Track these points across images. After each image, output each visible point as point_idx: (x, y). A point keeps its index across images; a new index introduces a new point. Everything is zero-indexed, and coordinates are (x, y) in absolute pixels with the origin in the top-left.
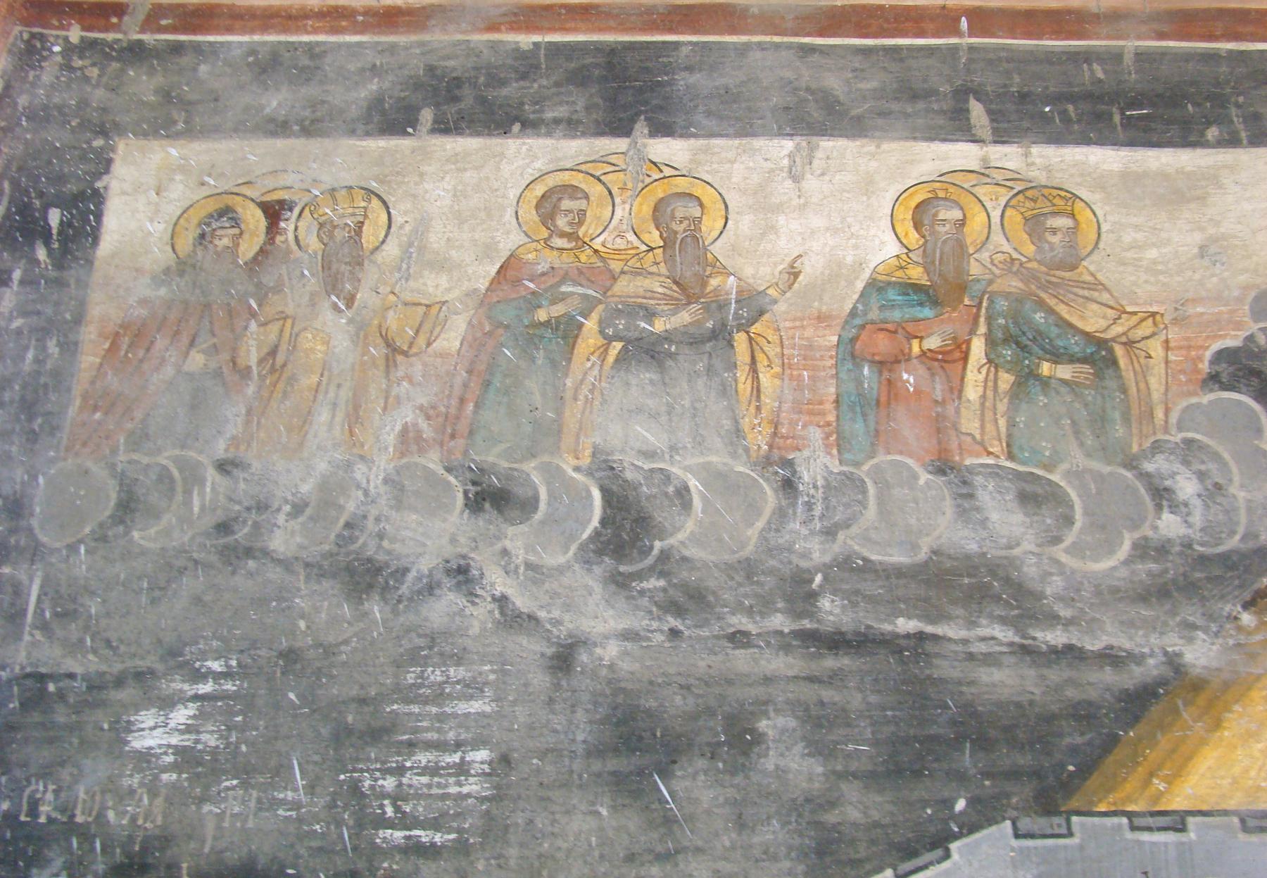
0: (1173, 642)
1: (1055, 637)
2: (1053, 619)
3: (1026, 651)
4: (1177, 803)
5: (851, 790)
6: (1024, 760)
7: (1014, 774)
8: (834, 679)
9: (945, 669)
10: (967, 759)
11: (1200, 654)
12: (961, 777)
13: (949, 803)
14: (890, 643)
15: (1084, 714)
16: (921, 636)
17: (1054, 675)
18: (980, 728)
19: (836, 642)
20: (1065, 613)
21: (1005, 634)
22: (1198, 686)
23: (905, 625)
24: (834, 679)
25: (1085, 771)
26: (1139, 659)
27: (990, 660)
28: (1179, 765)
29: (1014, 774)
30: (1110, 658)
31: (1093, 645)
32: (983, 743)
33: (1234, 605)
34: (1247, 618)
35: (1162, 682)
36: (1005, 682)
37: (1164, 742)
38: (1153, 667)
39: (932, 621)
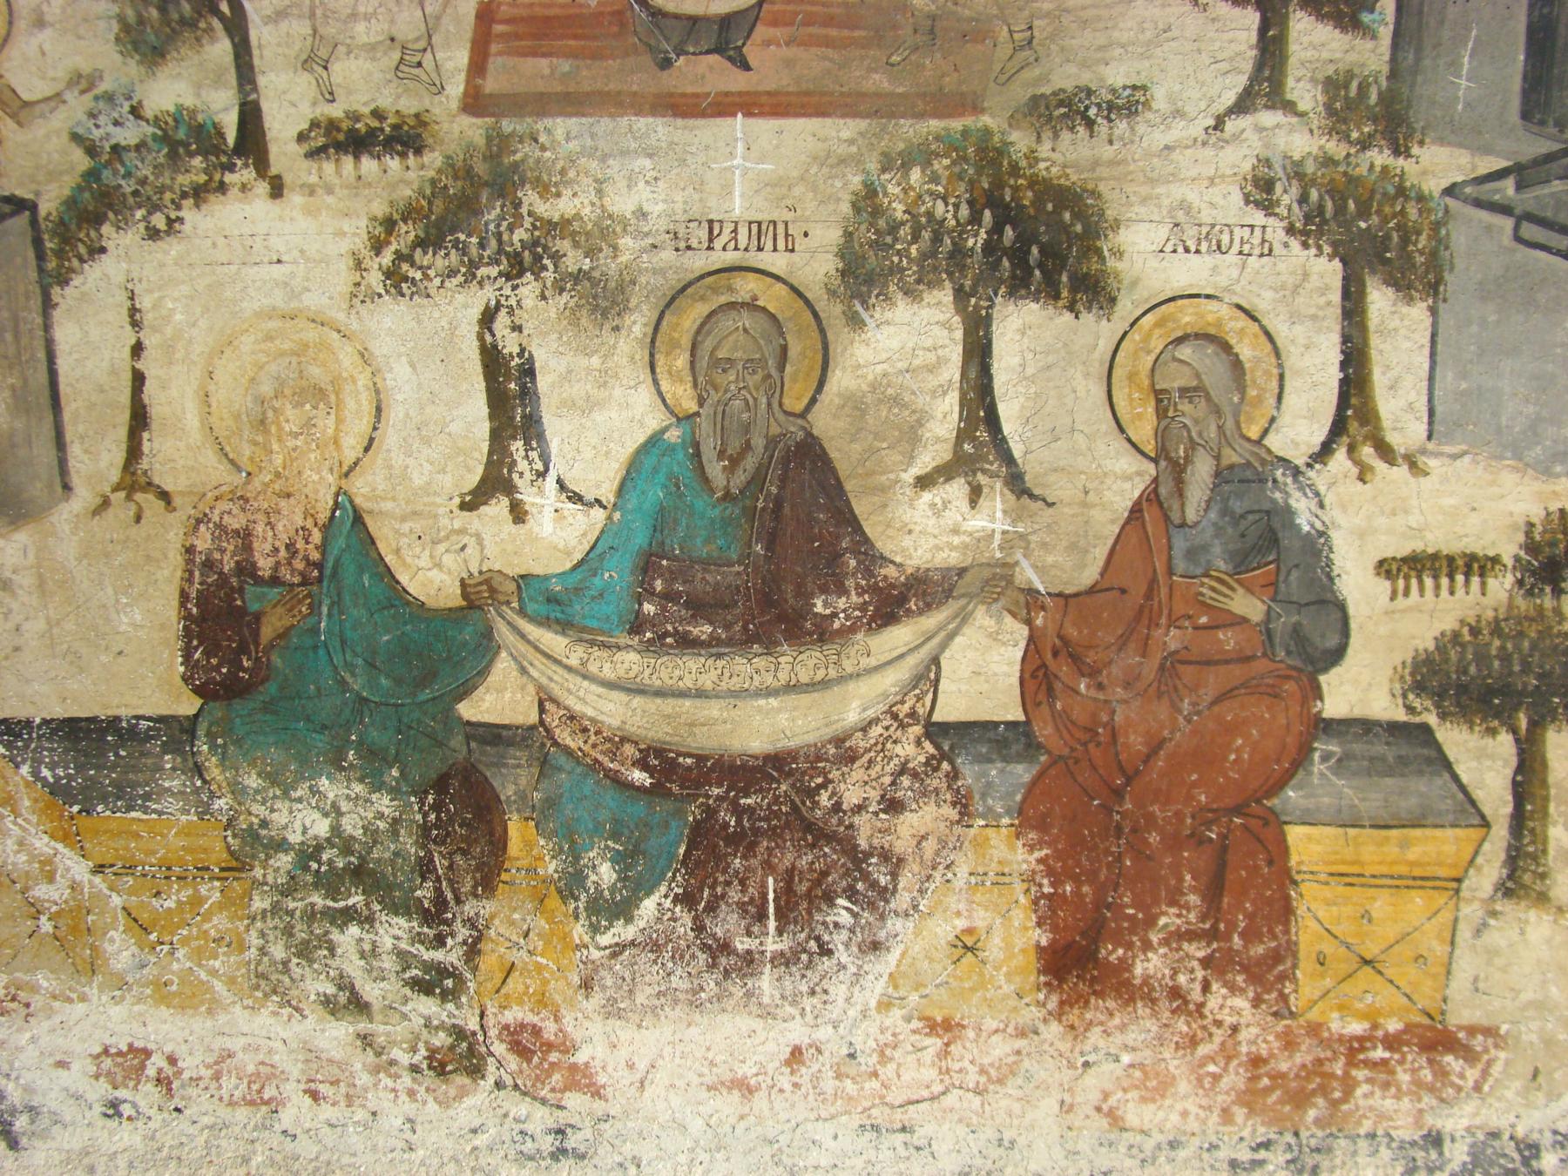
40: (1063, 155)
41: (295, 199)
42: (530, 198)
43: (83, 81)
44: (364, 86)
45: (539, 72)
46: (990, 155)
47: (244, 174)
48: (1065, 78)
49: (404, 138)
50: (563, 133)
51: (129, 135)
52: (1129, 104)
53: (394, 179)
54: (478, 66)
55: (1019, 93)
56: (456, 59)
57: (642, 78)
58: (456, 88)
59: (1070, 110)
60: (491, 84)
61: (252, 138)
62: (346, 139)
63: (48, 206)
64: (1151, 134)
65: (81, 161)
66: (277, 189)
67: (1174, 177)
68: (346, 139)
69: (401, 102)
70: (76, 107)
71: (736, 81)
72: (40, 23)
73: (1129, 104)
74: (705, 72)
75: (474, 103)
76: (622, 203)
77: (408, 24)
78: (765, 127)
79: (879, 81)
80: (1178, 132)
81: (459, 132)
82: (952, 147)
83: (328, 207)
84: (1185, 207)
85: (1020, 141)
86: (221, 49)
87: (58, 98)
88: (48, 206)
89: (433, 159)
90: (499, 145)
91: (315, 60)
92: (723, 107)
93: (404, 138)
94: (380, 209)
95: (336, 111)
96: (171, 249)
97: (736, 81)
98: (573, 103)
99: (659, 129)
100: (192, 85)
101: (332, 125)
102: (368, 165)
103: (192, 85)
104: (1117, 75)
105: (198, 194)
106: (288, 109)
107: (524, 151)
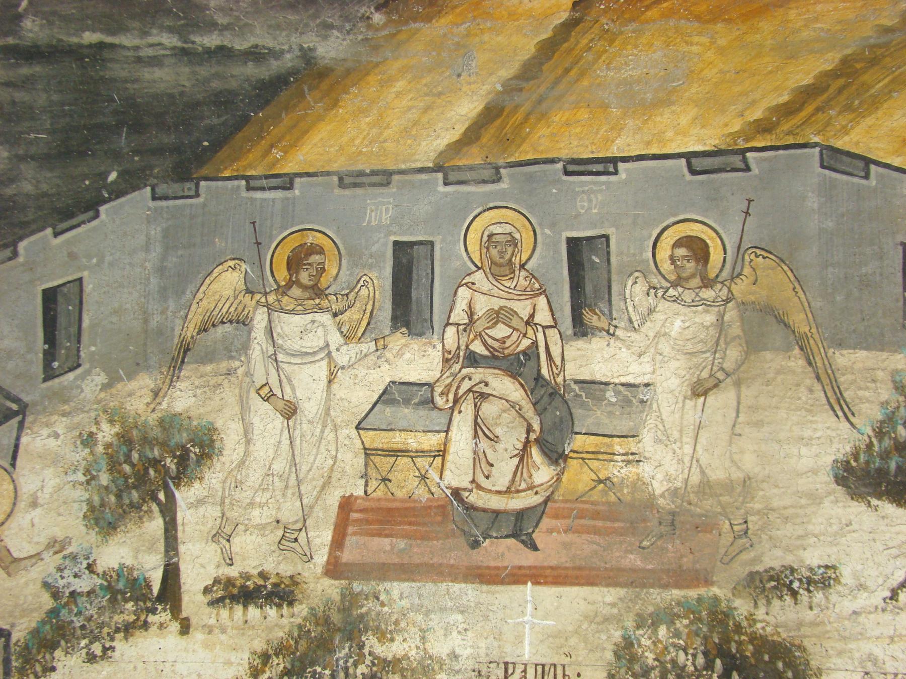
0: (310, 40)
1: (211, 40)
2: (212, 26)
3: (184, 54)
4: (289, 167)
5: (28, 170)
6: (168, 139)
7: (159, 151)
8: (26, 83)
9: (117, 71)
10: (123, 141)
11: (330, 48)
12: (116, 156)
13: (104, 175)
14: (74, 53)
15: (223, 100)
16: (101, 46)
17: (204, 71)
18: (138, 115)
19: (32, 54)
20: (222, 20)
21: (170, 40)
22: (323, 73)
23: (90, 37)
24: (26, 83)
25: (217, 146)
26: (276, 54)
27: (155, 62)
28: (298, 134)
29: (159, 151)
30: (255, 55)
31: (241, 45)
32: (137, 128)
33: (369, 7)
34: (378, 18)
35: (294, 72)
36: (165, 78)
37: (287, 120)
38: (289, 60)
39: (113, 33)
40: (775, 618)
41: (198, 636)
42: (371, 642)
43: (57, 545)
44: (255, 555)
45: (382, 548)
46: (719, 617)
47: (163, 616)
48: (774, 559)
49: (281, 594)
50: (397, 593)
51: (83, 585)
52: (823, 579)
53: (271, 623)
54: (338, 542)
55: (740, 570)
56: (322, 537)
57: (457, 554)
58: (321, 558)
59: (779, 583)
60: (347, 556)
61: (171, 590)
62: (239, 593)
63: (18, 635)
64: (841, 603)
65: (47, 602)
66: (185, 628)
67: (862, 635)
68: (239, 593)
69: (281, 567)
70: (51, 561)
71: (527, 558)
72: (34, 504)
73: (823, 579)
74: (505, 551)
75: (334, 569)
76: (439, 647)
77: (290, 511)
78: (548, 592)
79: (634, 560)
80: (862, 600)
81: (321, 589)
82: (690, 610)
83: (221, 643)
84: (874, 660)
85: (742, 607)
86: (156, 525)
87: (38, 556)
88: (18, 635)
89: (301, 609)
90: (350, 600)
91: (222, 535)
92: (517, 577)
93: (281, 594)
94: (259, 645)
95: (233, 572)
96: (103, 669)
97: (527, 558)
98: (405, 571)
99: (470, 592)
100: (133, 551)
101: (230, 582)
102: (253, 612)
103: (133, 551)
104: (813, 558)
105: (128, 629)
106: (199, 568)
107: (369, 605)
